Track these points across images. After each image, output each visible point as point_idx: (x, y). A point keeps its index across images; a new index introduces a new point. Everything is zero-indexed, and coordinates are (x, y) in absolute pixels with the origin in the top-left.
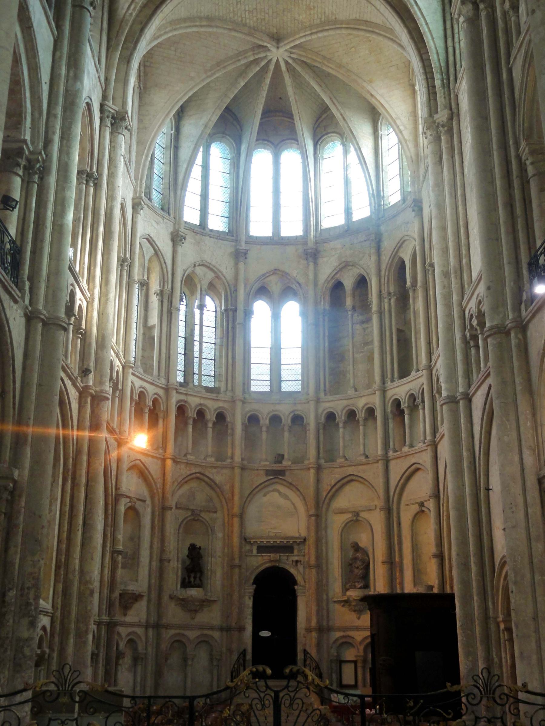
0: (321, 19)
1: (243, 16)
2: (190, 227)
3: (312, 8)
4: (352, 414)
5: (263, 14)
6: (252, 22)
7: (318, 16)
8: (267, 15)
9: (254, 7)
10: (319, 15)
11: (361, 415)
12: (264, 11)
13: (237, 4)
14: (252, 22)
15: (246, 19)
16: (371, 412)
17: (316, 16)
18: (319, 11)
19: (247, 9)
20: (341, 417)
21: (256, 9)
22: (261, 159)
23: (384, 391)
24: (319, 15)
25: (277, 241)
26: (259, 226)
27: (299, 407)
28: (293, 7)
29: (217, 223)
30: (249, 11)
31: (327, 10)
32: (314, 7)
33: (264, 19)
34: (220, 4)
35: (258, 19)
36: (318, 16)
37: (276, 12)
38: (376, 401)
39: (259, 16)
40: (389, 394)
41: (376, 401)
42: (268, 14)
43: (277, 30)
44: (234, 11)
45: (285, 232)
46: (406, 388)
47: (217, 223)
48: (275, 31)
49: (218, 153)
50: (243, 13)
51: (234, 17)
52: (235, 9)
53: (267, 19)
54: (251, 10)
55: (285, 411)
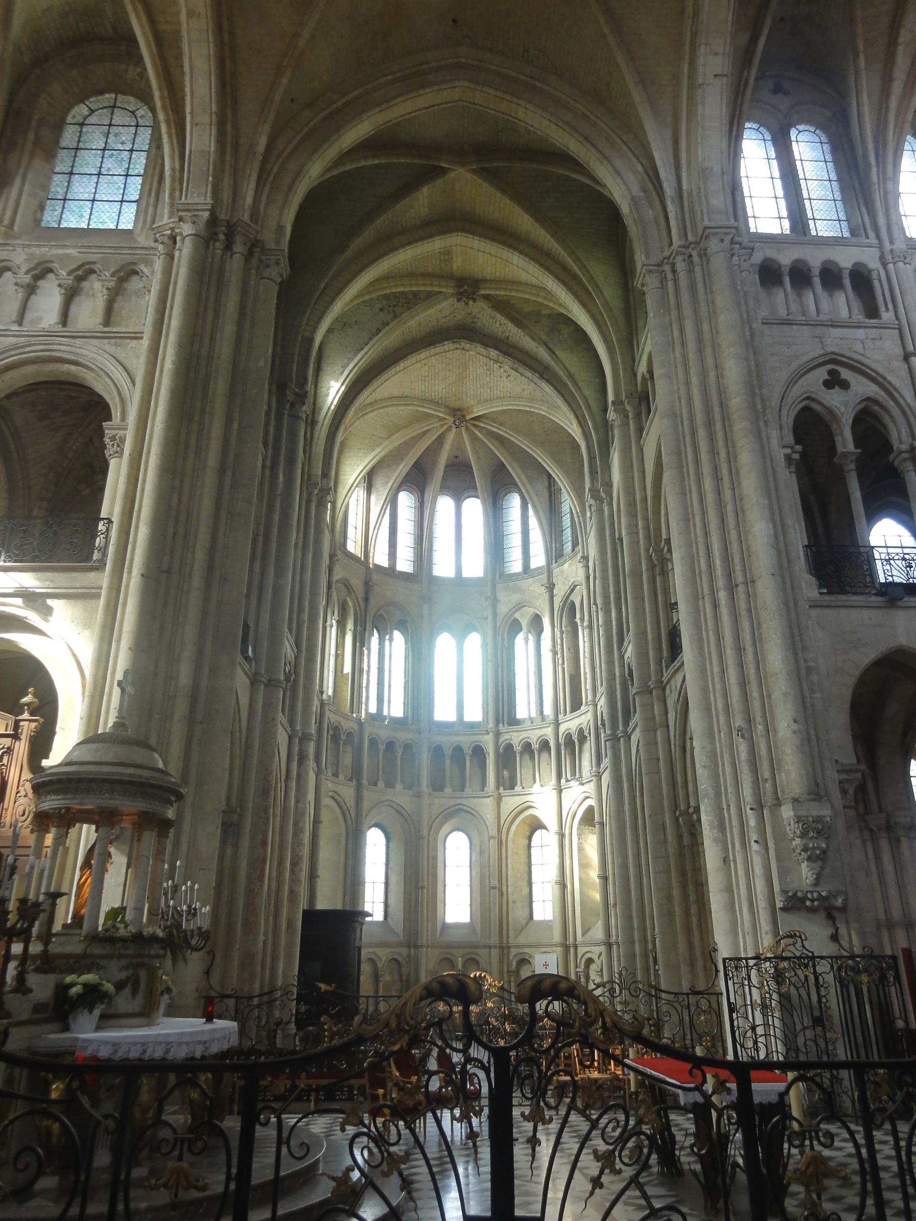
2: (378, 568)
4: (527, 747)
11: (535, 746)
16: (545, 745)
20: (518, 748)
22: (445, 505)
23: (557, 724)
25: (459, 581)
26: (443, 567)
27: (479, 738)
29: (404, 565)
38: (549, 732)
40: (562, 728)
41: (549, 732)
45: (466, 574)
46: (577, 722)
47: (404, 565)
49: (406, 500)
55: (466, 742)
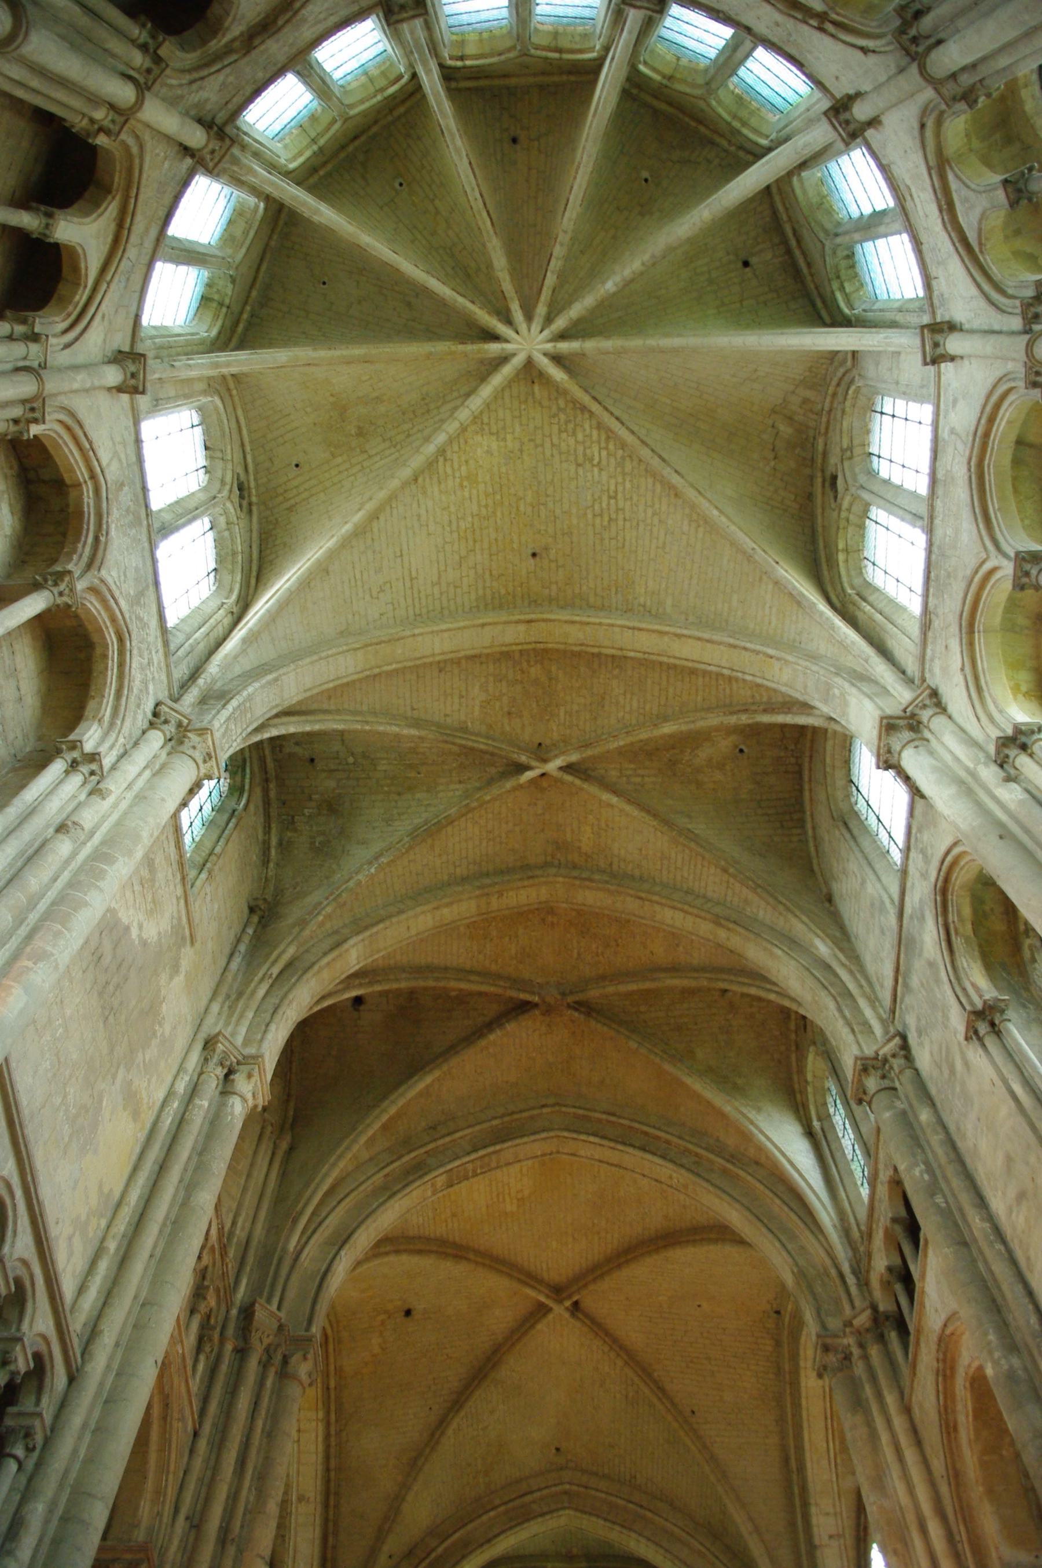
0: (445, 460)
1: (604, 453)
3: (465, 483)
5: (563, 444)
6: (587, 426)
7: (452, 466)
8: (555, 440)
9: (581, 471)
10: (449, 470)
12: (560, 453)
13: (616, 492)
14: (587, 426)
15: (599, 442)
17: (456, 466)
18: (450, 483)
19: (596, 470)
21: (578, 465)
24: (449, 470)
28: (503, 470)
30: (591, 460)
31: (436, 489)
32: (462, 486)
33: (560, 431)
34: (650, 511)
35: (574, 434)
36: (452, 466)
37: (536, 446)
39: (572, 441)
42: (553, 445)
43: (533, 394)
44: (624, 474)
48: (536, 388)
50: (604, 462)
51: (623, 458)
52: (620, 480)
53: (555, 428)
54: (588, 466)
